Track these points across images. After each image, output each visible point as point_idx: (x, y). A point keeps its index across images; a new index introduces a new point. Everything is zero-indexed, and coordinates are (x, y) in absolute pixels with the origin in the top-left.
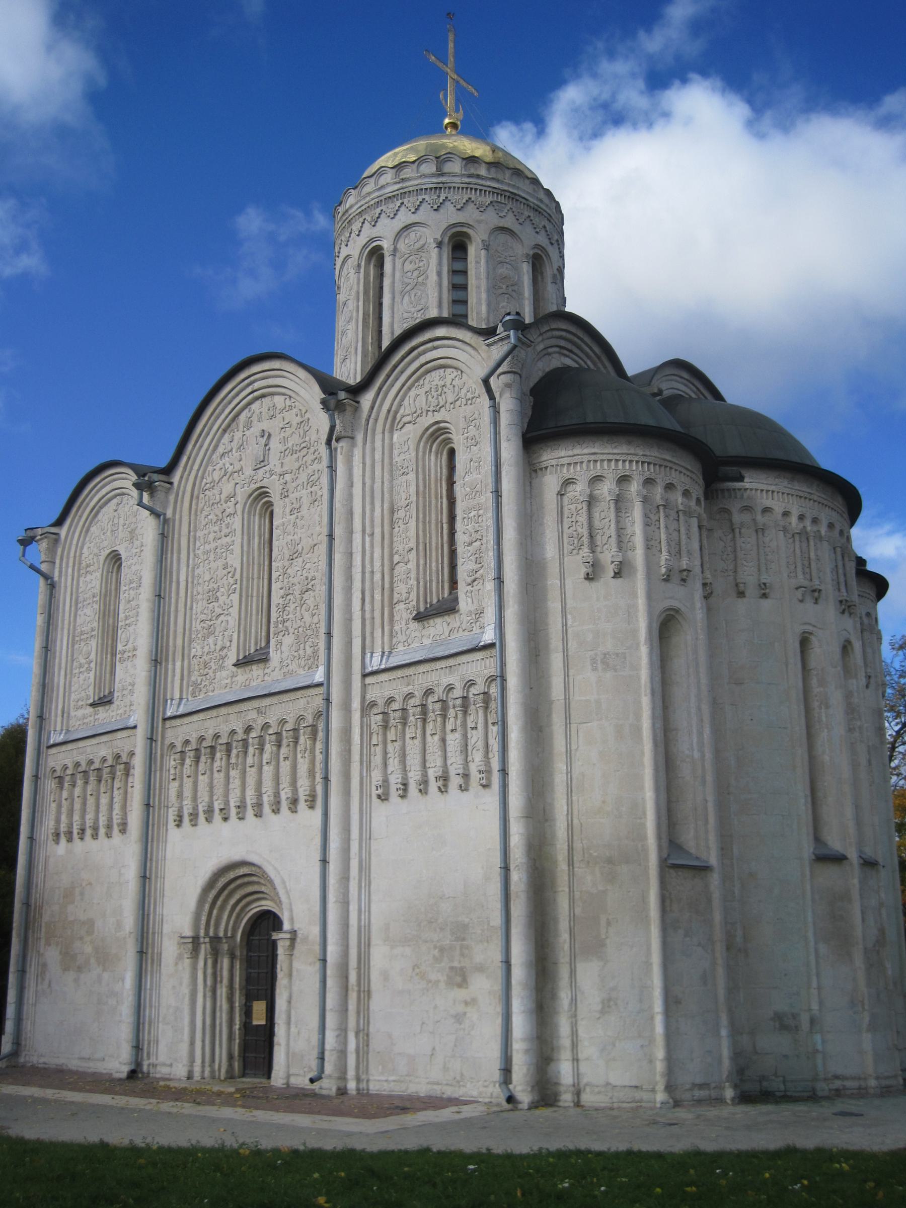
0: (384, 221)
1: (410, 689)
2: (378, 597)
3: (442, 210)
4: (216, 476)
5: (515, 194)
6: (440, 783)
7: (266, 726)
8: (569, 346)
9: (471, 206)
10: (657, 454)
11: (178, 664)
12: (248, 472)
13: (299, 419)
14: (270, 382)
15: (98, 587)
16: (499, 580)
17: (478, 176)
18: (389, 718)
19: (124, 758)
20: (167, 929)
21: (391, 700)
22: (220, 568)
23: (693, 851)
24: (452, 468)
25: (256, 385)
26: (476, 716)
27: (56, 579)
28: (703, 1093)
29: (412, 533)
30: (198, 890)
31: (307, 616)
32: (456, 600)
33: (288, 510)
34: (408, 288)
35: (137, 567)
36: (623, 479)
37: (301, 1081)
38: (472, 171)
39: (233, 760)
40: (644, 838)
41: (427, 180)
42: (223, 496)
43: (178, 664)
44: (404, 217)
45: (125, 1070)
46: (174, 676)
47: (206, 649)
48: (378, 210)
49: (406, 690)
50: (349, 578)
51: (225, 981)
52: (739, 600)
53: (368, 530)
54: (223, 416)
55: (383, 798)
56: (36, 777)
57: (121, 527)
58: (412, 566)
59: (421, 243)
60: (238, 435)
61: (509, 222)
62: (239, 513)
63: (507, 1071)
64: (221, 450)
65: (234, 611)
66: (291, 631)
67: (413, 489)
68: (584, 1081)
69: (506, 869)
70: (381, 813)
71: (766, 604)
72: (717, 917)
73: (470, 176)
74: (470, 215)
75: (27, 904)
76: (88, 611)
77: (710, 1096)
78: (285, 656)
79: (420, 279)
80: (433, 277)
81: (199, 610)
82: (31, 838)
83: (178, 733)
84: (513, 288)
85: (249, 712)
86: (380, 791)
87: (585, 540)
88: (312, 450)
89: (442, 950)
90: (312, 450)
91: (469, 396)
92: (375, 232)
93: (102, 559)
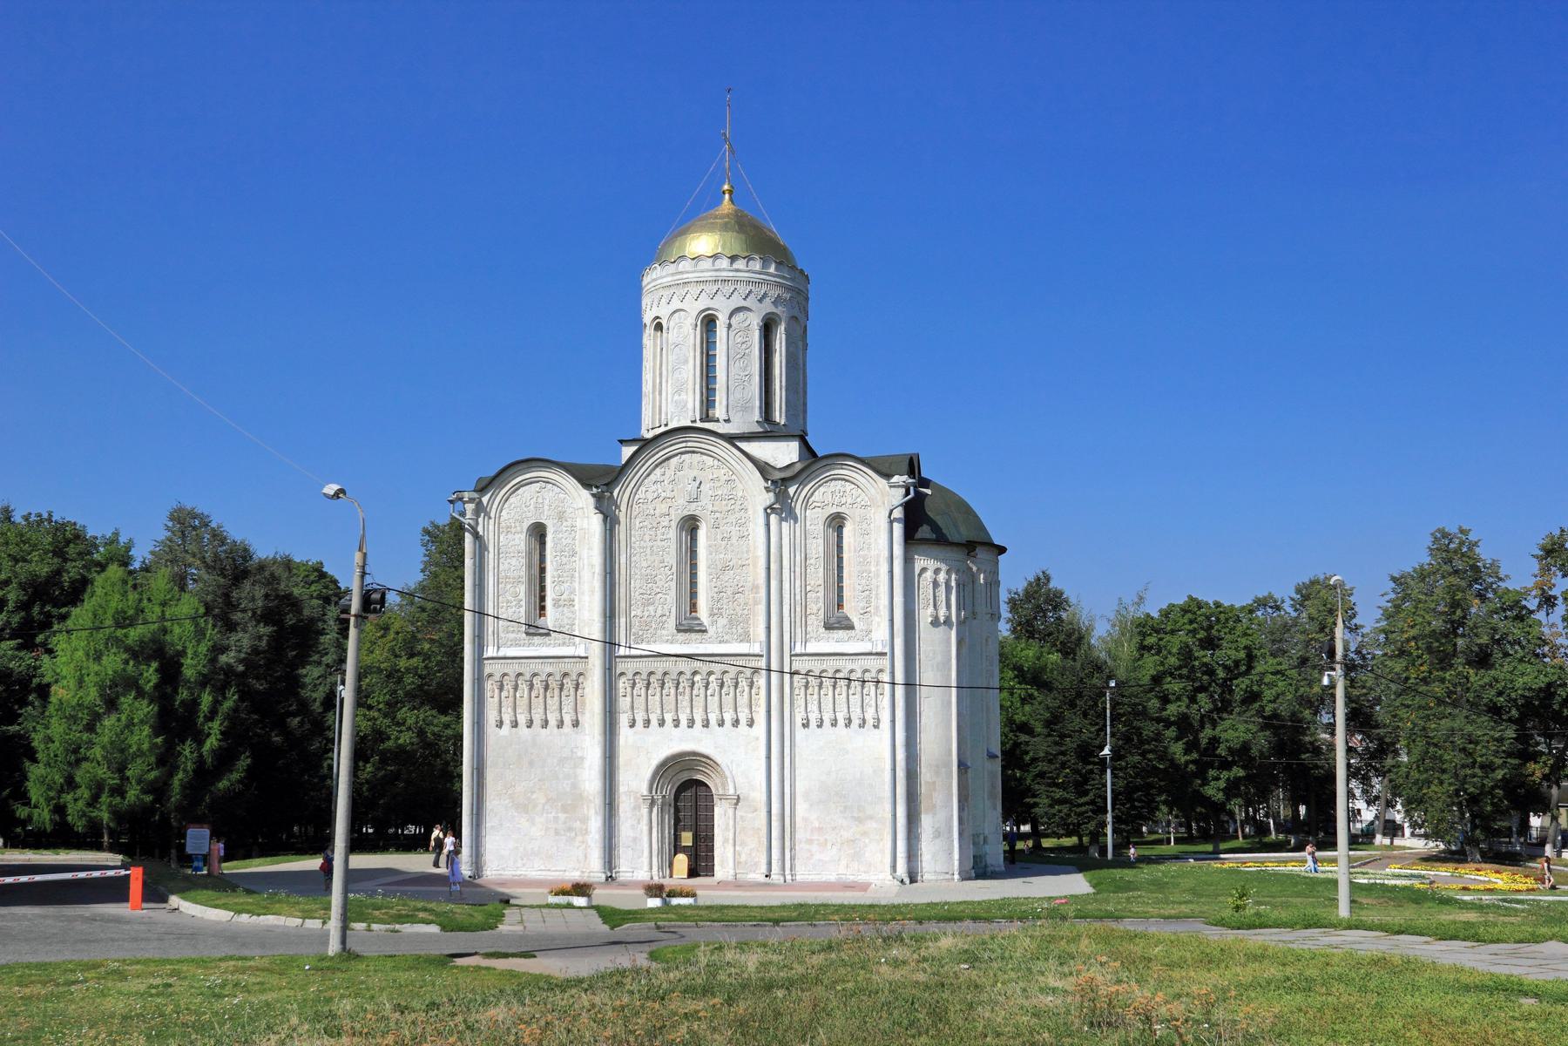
0: (719, 297)
12: (681, 501)
16: (892, 621)
24: (840, 537)
29: (821, 574)
32: (847, 618)
33: (719, 537)
36: (948, 572)
37: (731, 878)
43: (623, 620)
44: (737, 301)
55: (806, 725)
56: (479, 681)
58: (821, 594)
60: (670, 473)
65: (673, 593)
67: (821, 549)
69: (894, 770)
74: (779, 310)
76: (514, 561)
85: (697, 665)
92: (711, 304)
93: (526, 525)
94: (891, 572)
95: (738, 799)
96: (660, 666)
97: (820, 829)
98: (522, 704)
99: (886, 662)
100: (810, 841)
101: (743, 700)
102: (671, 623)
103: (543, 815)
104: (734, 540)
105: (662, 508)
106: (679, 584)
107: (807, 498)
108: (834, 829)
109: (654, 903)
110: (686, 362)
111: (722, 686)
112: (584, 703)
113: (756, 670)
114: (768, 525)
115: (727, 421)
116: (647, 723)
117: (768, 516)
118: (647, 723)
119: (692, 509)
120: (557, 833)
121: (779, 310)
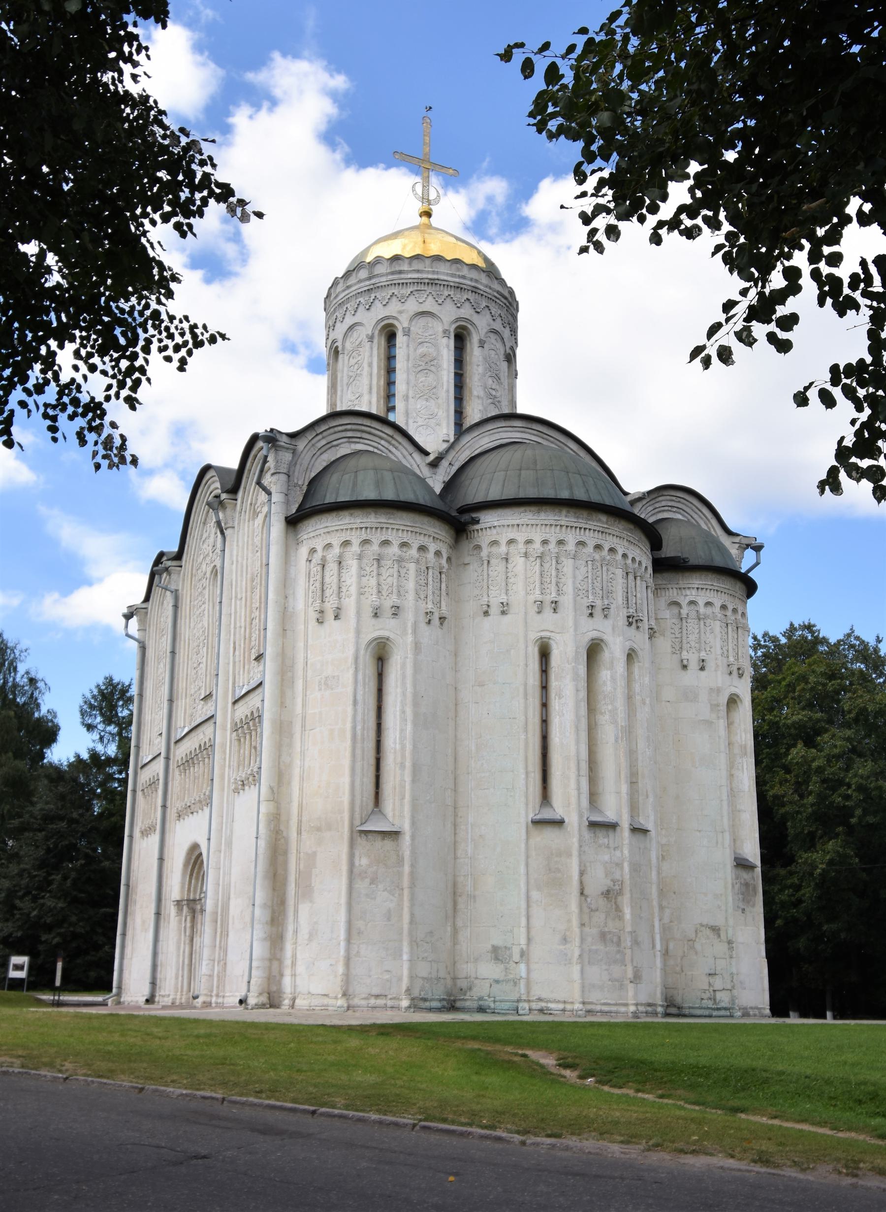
3: (372, 309)
5: (434, 279)
8: (359, 435)
9: (394, 299)
10: (373, 520)
17: (400, 272)
23: (391, 820)
28: (380, 1002)
38: (397, 269)
41: (362, 284)
52: (486, 618)
56: (134, 791)
68: (298, 990)
71: (506, 619)
72: (407, 869)
73: (393, 273)
77: (386, 1004)
83: (181, 751)
84: (432, 363)
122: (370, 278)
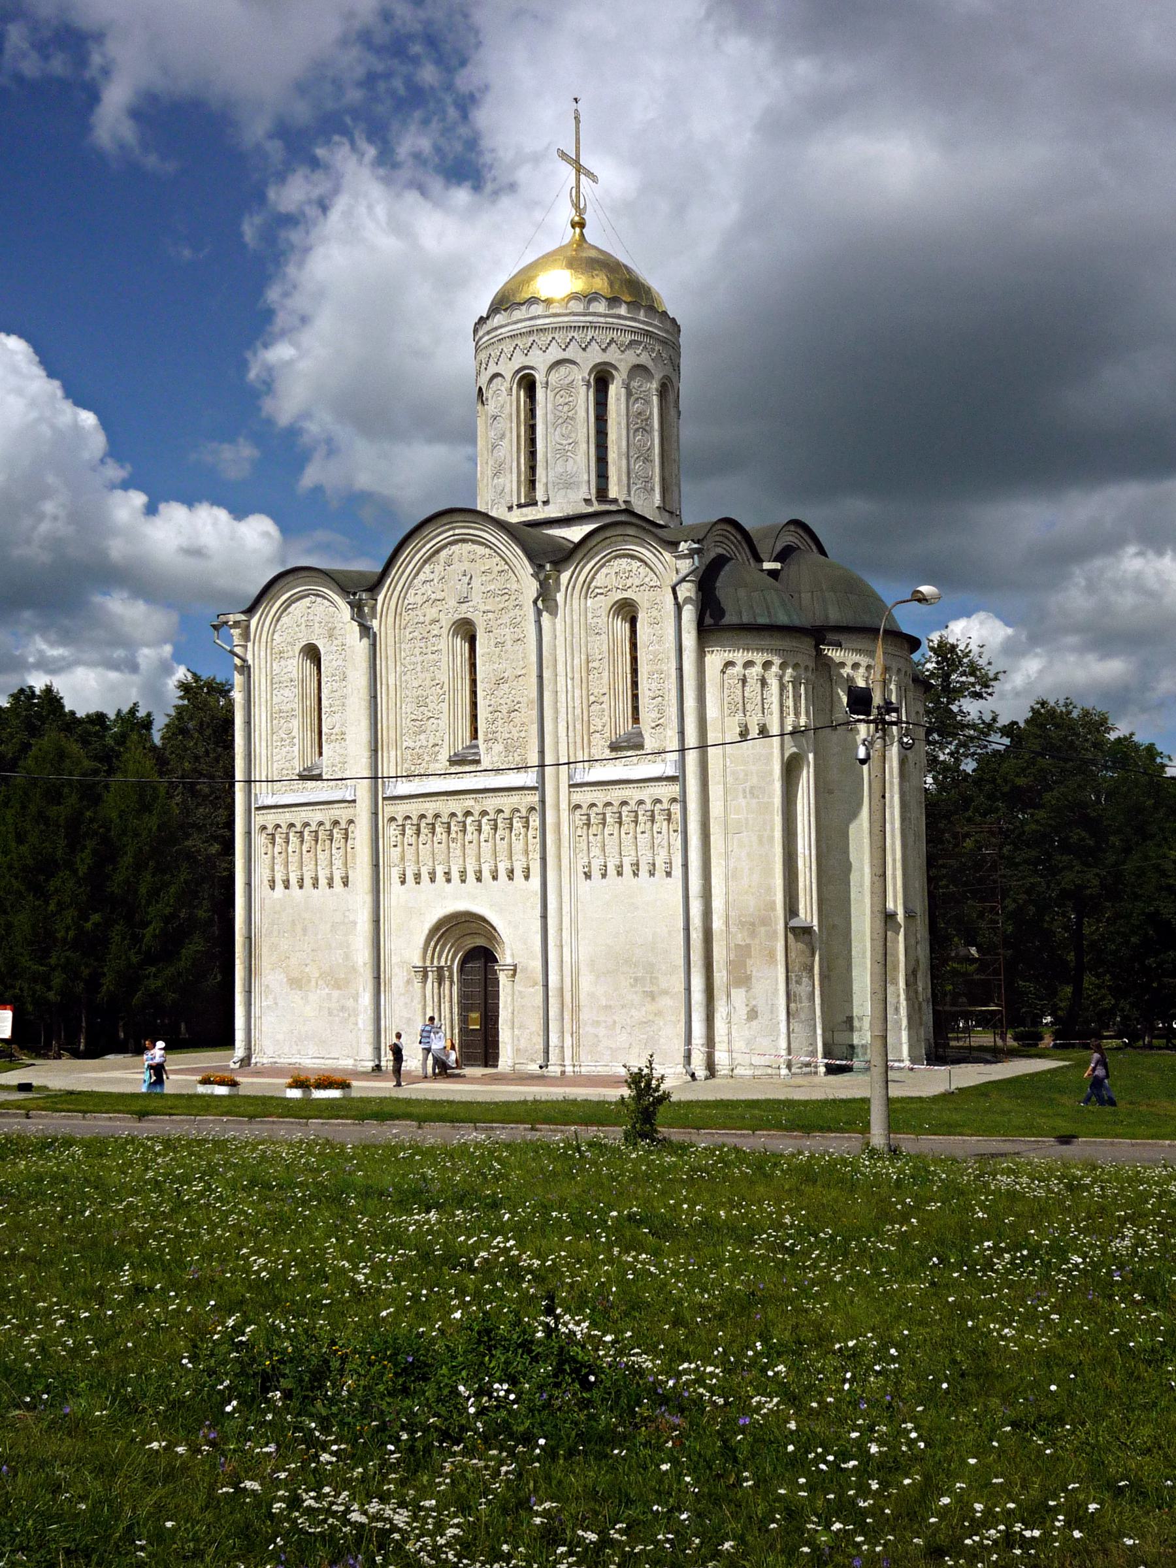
0: (535, 351)
1: (608, 799)
2: (578, 726)
4: (419, 600)
6: (634, 868)
7: (484, 813)
11: (393, 753)
12: (452, 603)
13: (499, 568)
14: (471, 531)
15: (295, 672)
17: (619, 317)
18: (590, 819)
19: (343, 825)
20: (395, 959)
21: (593, 805)
22: (428, 679)
25: (457, 531)
26: (661, 823)
27: (250, 662)
29: (605, 680)
30: (426, 932)
31: (514, 731)
32: (640, 735)
33: (492, 643)
34: (560, 421)
35: (340, 662)
36: (767, 665)
39: (453, 835)
40: (774, 909)
42: (428, 619)
43: (393, 753)
44: (555, 354)
45: (371, 1064)
46: (389, 762)
47: (418, 744)
48: (531, 339)
49: (606, 800)
50: (556, 711)
51: (447, 998)
53: (569, 675)
54: (424, 550)
56: (248, 833)
57: (317, 625)
59: (570, 379)
60: (439, 568)
61: (644, 359)
62: (445, 636)
63: (688, 1057)
64: (422, 577)
65: (444, 717)
66: (501, 740)
67: (605, 647)
70: (584, 886)
75: (249, 938)
76: (287, 692)
78: (495, 759)
79: (570, 414)
80: (582, 414)
81: (409, 711)
82: (248, 884)
85: (469, 802)
86: (586, 870)
87: (740, 706)
88: (513, 597)
89: (636, 979)
90: (513, 597)
91: (652, 584)
94: (680, 669)
95: (515, 970)
96: (430, 807)
97: (608, 1007)
98: (294, 859)
99: (674, 789)
100: (597, 1023)
101: (518, 846)
102: (444, 756)
103: (319, 989)
104: (509, 643)
105: (432, 612)
106: (453, 705)
107: (587, 584)
108: (623, 1007)
109: (296, 1093)
110: (502, 437)
111: (495, 829)
112: (354, 856)
113: (533, 809)
114: (538, 622)
115: (546, 503)
116: (418, 877)
117: (539, 613)
118: (418, 877)
119: (464, 612)
120: (330, 1014)
121: (613, 355)
122: (585, 315)
